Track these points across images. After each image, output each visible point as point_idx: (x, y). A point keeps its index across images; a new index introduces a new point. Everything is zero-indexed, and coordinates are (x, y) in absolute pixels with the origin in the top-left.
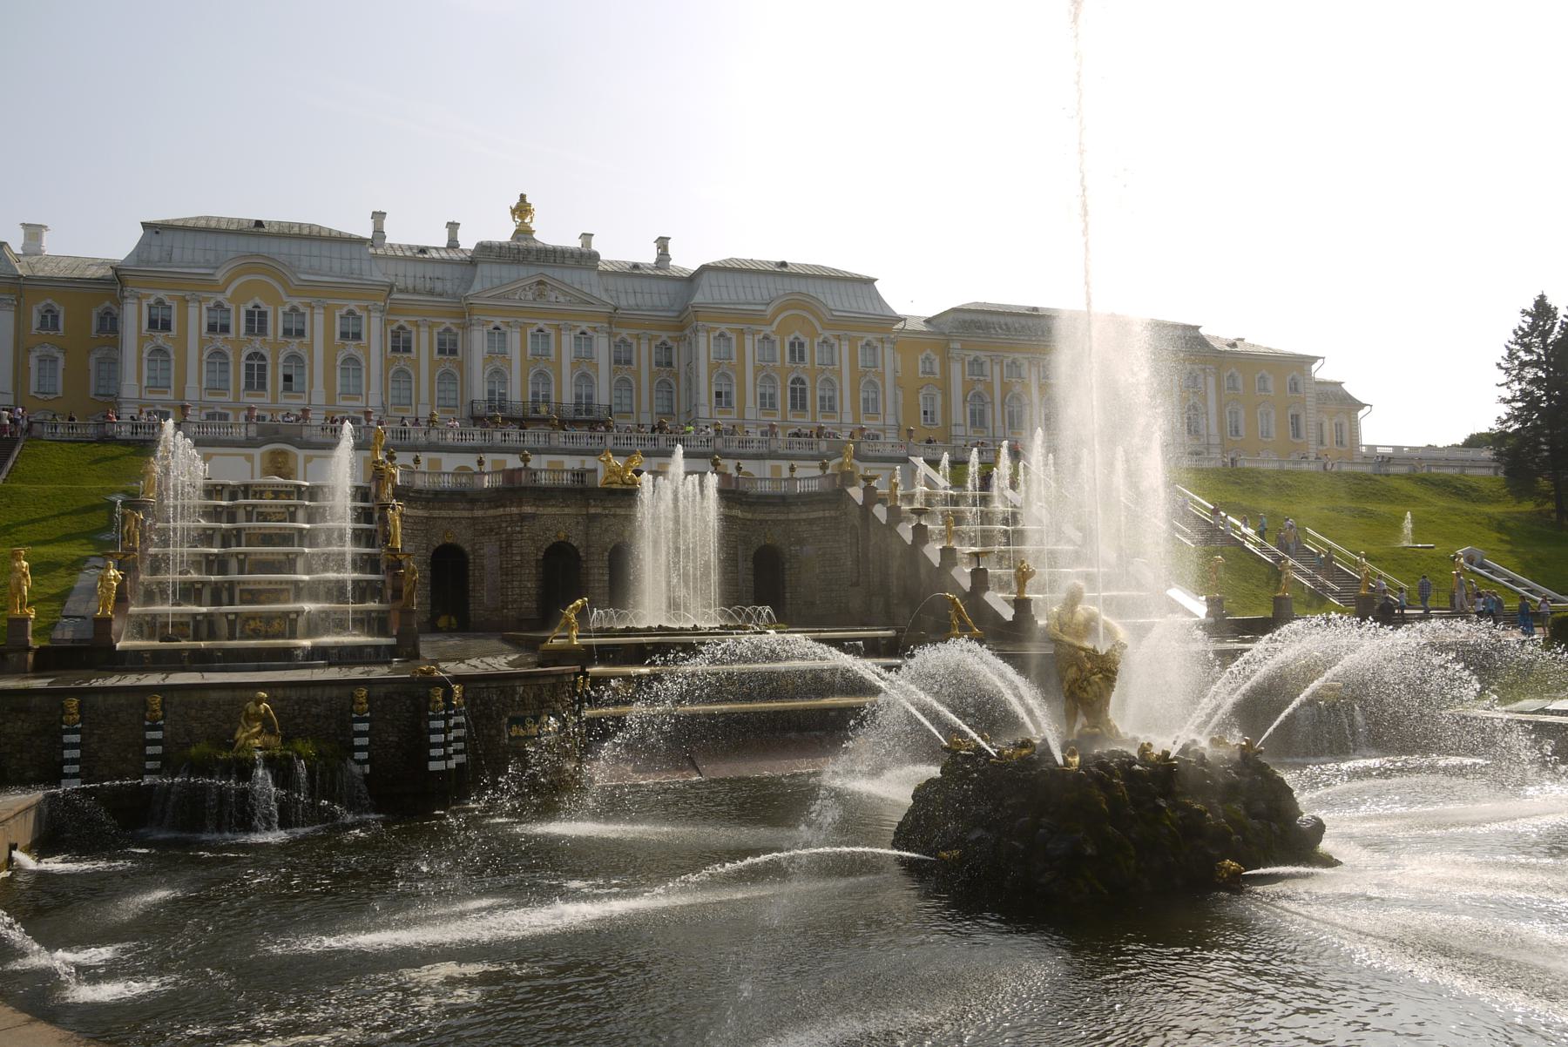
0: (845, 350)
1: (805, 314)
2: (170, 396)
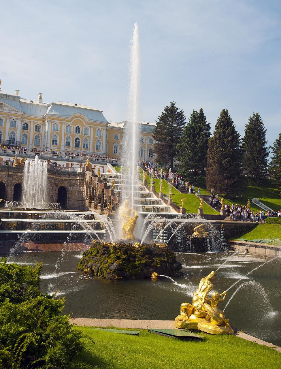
1: (80, 119)
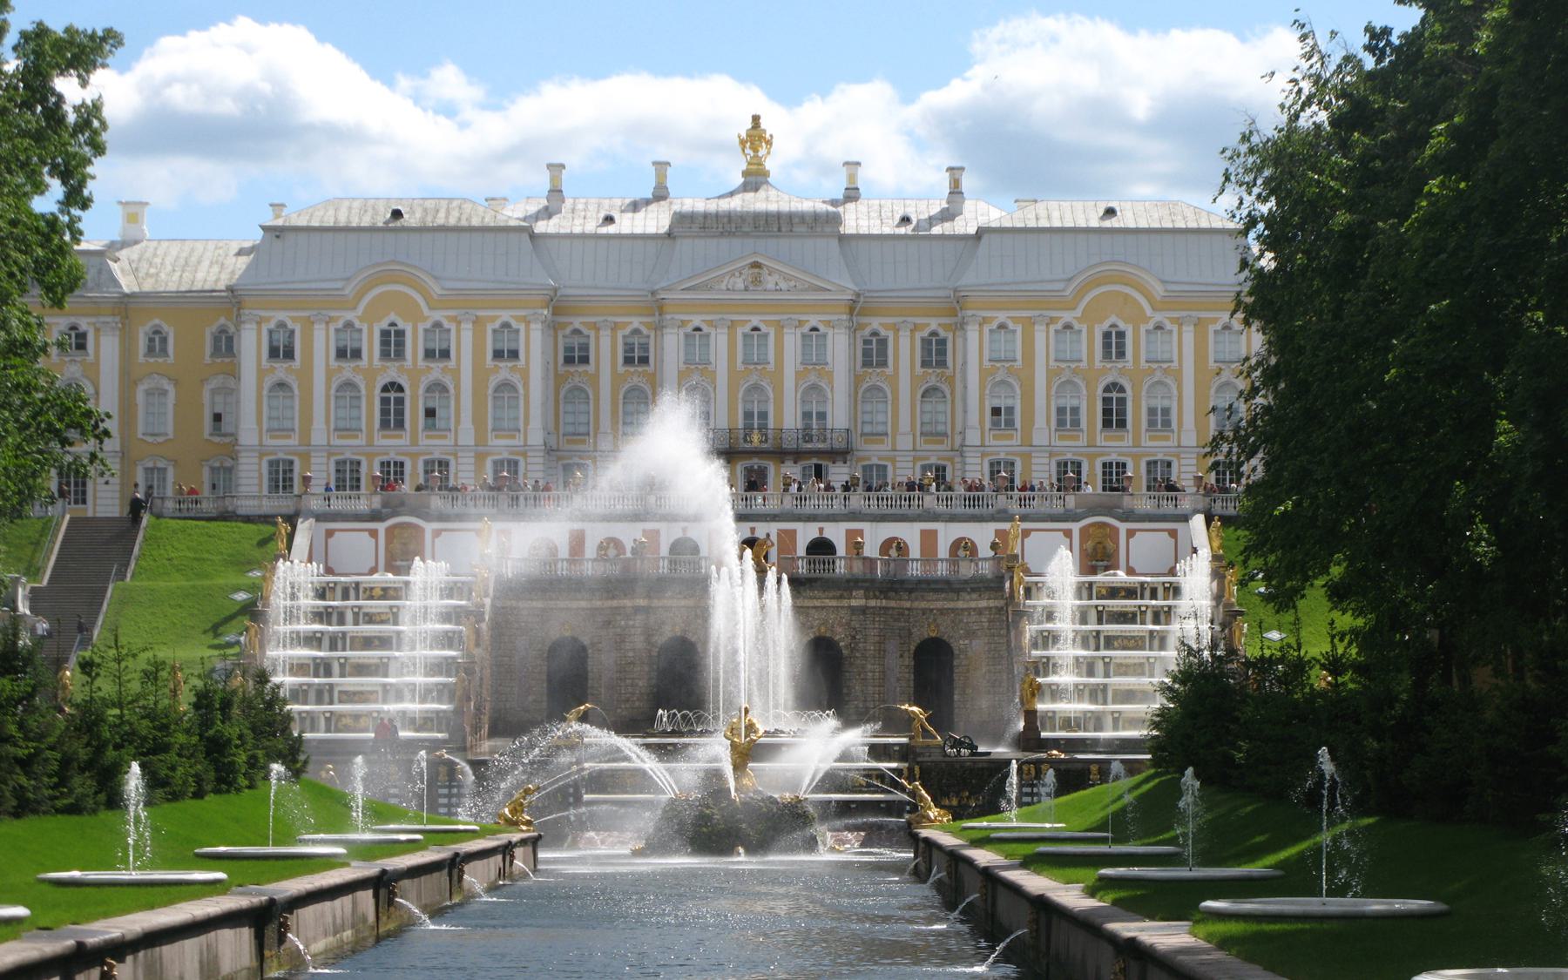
1: (1127, 290)
2: (294, 441)
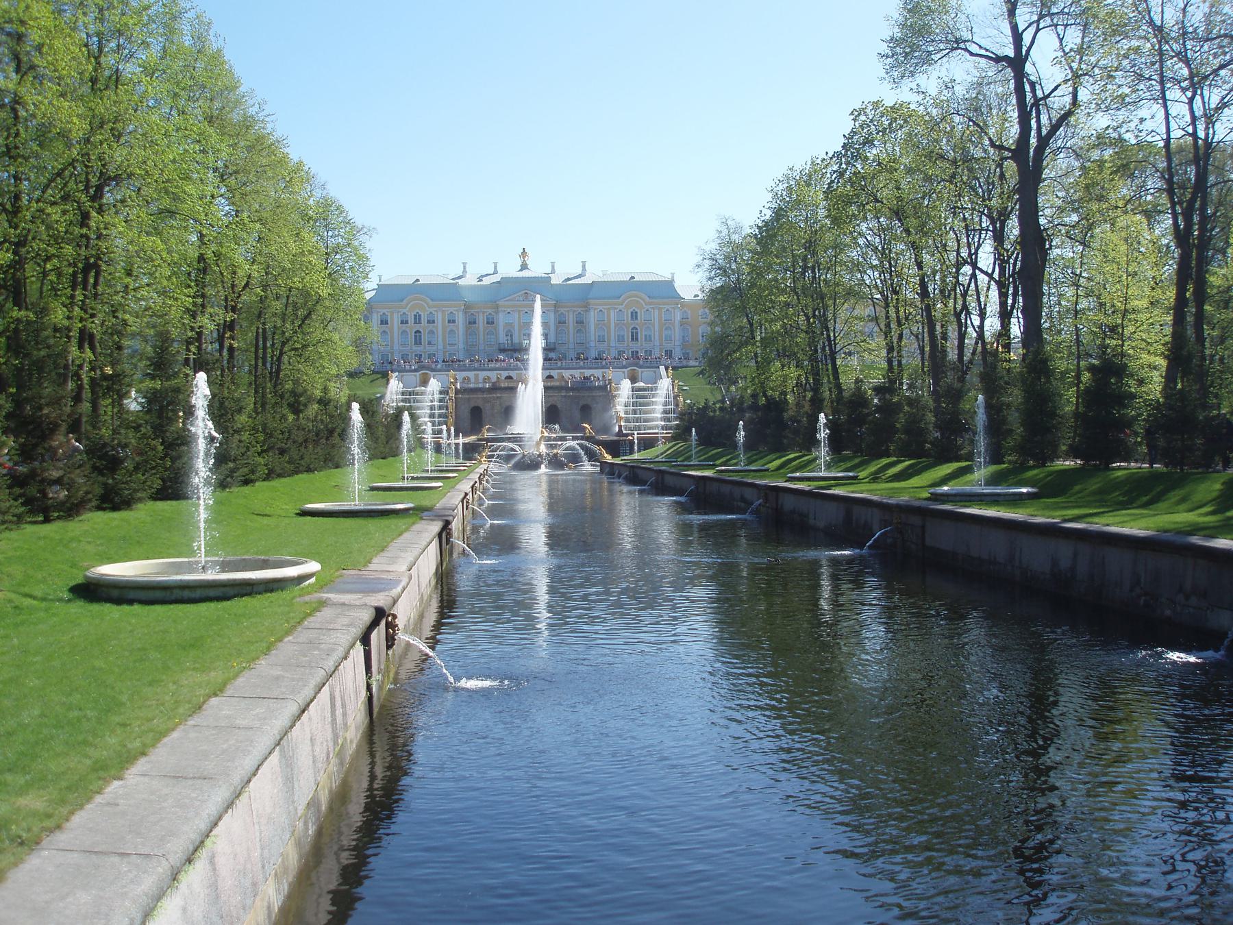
0: (657, 312)
